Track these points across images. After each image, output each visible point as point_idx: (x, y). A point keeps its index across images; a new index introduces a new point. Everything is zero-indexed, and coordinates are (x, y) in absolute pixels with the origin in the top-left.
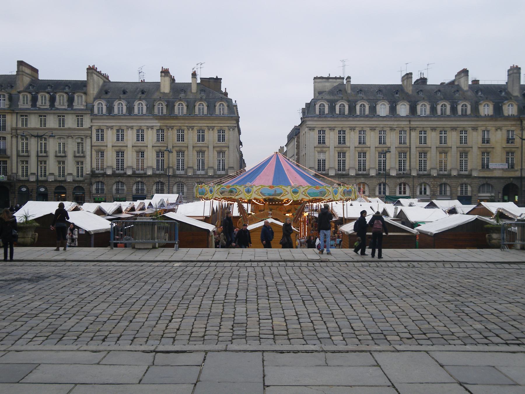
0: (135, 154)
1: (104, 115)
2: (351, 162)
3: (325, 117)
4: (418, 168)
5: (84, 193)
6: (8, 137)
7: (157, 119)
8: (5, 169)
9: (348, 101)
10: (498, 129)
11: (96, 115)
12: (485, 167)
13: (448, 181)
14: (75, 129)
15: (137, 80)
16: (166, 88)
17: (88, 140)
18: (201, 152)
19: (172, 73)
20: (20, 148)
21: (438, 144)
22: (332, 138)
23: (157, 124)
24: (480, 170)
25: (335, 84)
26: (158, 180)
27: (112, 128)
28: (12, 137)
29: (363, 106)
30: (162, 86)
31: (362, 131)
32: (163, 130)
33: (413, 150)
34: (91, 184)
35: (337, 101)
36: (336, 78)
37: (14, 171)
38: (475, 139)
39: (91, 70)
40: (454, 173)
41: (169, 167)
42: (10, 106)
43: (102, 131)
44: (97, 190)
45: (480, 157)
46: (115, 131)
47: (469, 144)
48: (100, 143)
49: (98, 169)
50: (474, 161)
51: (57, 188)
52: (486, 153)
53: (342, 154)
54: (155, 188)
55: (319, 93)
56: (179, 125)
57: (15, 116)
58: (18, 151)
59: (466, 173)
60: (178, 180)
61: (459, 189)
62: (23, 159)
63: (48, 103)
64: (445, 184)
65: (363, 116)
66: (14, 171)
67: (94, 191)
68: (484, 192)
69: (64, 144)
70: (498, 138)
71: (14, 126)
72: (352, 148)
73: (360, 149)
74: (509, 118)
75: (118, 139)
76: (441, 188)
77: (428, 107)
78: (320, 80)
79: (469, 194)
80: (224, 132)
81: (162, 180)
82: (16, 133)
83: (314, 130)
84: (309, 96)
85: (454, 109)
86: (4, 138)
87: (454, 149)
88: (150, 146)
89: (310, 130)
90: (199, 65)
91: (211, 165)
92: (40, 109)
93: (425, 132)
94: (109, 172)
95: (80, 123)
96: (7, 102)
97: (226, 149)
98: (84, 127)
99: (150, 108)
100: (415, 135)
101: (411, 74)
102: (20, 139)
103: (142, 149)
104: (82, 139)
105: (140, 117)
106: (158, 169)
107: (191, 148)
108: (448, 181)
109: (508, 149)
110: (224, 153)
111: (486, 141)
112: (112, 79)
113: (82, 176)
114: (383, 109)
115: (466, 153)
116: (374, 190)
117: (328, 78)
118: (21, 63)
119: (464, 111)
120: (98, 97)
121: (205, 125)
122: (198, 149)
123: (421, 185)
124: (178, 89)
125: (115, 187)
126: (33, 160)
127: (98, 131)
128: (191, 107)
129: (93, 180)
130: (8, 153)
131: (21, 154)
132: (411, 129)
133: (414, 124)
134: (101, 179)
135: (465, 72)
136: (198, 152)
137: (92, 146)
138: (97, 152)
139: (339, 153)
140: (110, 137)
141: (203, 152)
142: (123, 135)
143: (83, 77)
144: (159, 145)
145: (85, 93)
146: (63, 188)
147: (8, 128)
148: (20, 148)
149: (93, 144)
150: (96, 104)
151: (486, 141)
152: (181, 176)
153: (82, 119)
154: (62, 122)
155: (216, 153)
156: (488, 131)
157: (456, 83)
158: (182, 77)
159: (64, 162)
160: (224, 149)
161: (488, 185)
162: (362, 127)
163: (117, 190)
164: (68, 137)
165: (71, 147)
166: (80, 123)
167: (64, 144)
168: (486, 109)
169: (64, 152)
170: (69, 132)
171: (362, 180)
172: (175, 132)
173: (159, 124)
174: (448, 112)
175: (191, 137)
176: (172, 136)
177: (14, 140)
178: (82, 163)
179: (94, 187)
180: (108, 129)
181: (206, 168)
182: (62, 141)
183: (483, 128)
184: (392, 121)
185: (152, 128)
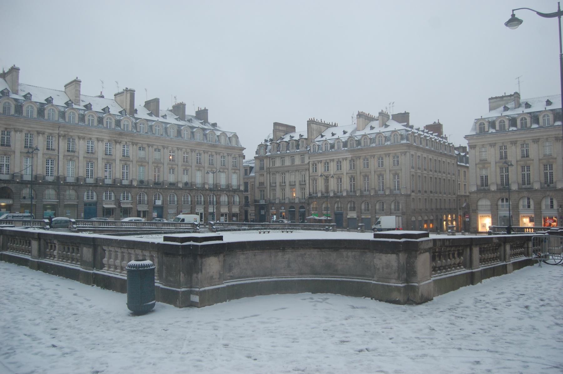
2: (515, 176)
6: (265, 174)
26: (350, 199)
27: (321, 162)
37: (268, 197)
54: (349, 206)
56: (364, 155)
58: (270, 183)
73: (522, 163)
78: (495, 100)
80: (398, 157)
81: (353, 199)
88: (345, 174)
95: (303, 161)
117: (503, 97)
118: (276, 124)
121: (383, 153)
126: (278, 188)
127: (313, 165)
130: (265, 185)
140: (321, 168)
144: (351, 172)
147: (265, 168)
162: (524, 141)
164: (296, 171)
166: (303, 161)
172: (362, 160)
173: (350, 156)
177: (268, 175)
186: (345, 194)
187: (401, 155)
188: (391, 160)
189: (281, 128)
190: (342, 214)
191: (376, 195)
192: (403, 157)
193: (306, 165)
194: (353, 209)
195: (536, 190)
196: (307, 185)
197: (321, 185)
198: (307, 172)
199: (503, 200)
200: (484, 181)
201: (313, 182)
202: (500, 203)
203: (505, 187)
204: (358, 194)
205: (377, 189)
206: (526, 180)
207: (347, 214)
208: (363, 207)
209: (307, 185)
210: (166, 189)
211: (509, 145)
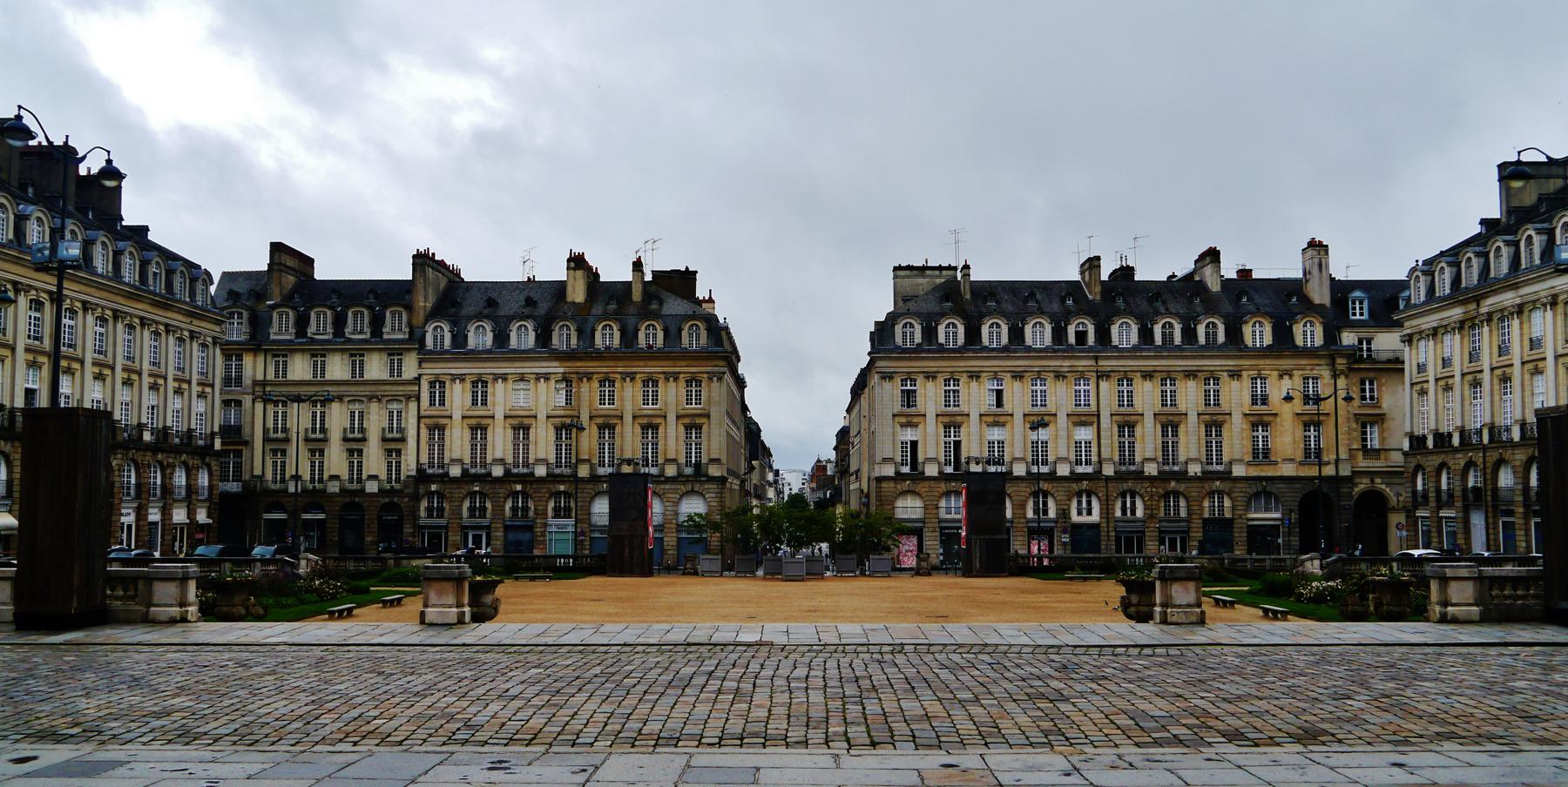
0: (510, 432)
1: (447, 352)
4: (1117, 458)
7: (556, 359)
8: (238, 467)
11: (430, 352)
12: (1262, 455)
13: (1182, 487)
15: (520, 277)
16: (577, 294)
17: (413, 406)
18: (650, 427)
19: (591, 260)
20: (270, 424)
21: (1158, 407)
22: (930, 396)
23: (556, 368)
24: (1249, 464)
25: (939, 281)
27: (462, 378)
28: (253, 401)
30: (569, 288)
34: (416, 498)
36: (940, 268)
38: (1236, 396)
39: (423, 261)
40: (1195, 469)
41: (579, 461)
42: (253, 336)
43: (442, 384)
44: (430, 510)
45: (1248, 434)
46: (468, 385)
49: (431, 465)
50: (1236, 442)
52: (1260, 422)
54: (551, 505)
55: (901, 298)
57: (261, 359)
59: (1220, 468)
61: (1206, 504)
63: (330, 330)
64: (1177, 494)
66: (258, 472)
69: (361, 414)
71: (260, 377)
75: (475, 402)
76: (1167, 501)
77: (1135, 329)
79: (1228, 515)
82: (265, 393)
83: (891, 378)
84: (882, 305)
85: (1189, 334)
86: (239, 403)
87: (1192, 418)
89: (883, 378)
90: (649, 245)
91: (671, 456)
92: (313, 341)
93: (1130, 381)
95: (395, 369)
96: (245, 328)
97: (704, 420)
98: (405, 376)
99: (544, 338)
101: (1098, 258)
106: (558, 464)
107: (628, 418)
108: (1182, 487)
109: (1306, 418)
110: (699, 427)
112: (467, 276)
113: (398, 480)
115: (1219, 426)
117: (923, 269)
118: (277, 249)
120: (436, 313)
122: (645, 421)
123: (1123, 495)
125: (466, 504)
127: (432, 384)
130: (246, 430)
131: (272, 435)
132: (1102, 375)
135: (1212, 255)
137: (419, 418)
138: (431, 429)
140: (458, 398)
141: (655, 428)
142: (485, 394)
143: (406, 273)
145: (409, 308)
146: (358, 506)
147: (247, 381)
149: (423, 413)
153: (400, 361)
154: (358, 368)
155: (682, 429)
156: (1264, 379)
157: (1197, 278)
158: (614, 270)
159: (360, 452)
161: (1268, 495)
164: (370, 398)
166: (395, 369)
167: (361, 414)
168: (1258, 333)
169: (362, 430)
170: (373, 388)
174: (1178, 339)
177: (259, 406)
178: (399, 452)
179: (424, 504)
180: (453, 380)
181: (661, 461)
182: (357, 407)
183: (1254, 373)
184: (1057, 358)
187: (710, 379)
189: (290, 262)
193: (409, 383)
195: (1018, 478)
196: (412, 442)
201: (431, 438)
209: (412, 442)
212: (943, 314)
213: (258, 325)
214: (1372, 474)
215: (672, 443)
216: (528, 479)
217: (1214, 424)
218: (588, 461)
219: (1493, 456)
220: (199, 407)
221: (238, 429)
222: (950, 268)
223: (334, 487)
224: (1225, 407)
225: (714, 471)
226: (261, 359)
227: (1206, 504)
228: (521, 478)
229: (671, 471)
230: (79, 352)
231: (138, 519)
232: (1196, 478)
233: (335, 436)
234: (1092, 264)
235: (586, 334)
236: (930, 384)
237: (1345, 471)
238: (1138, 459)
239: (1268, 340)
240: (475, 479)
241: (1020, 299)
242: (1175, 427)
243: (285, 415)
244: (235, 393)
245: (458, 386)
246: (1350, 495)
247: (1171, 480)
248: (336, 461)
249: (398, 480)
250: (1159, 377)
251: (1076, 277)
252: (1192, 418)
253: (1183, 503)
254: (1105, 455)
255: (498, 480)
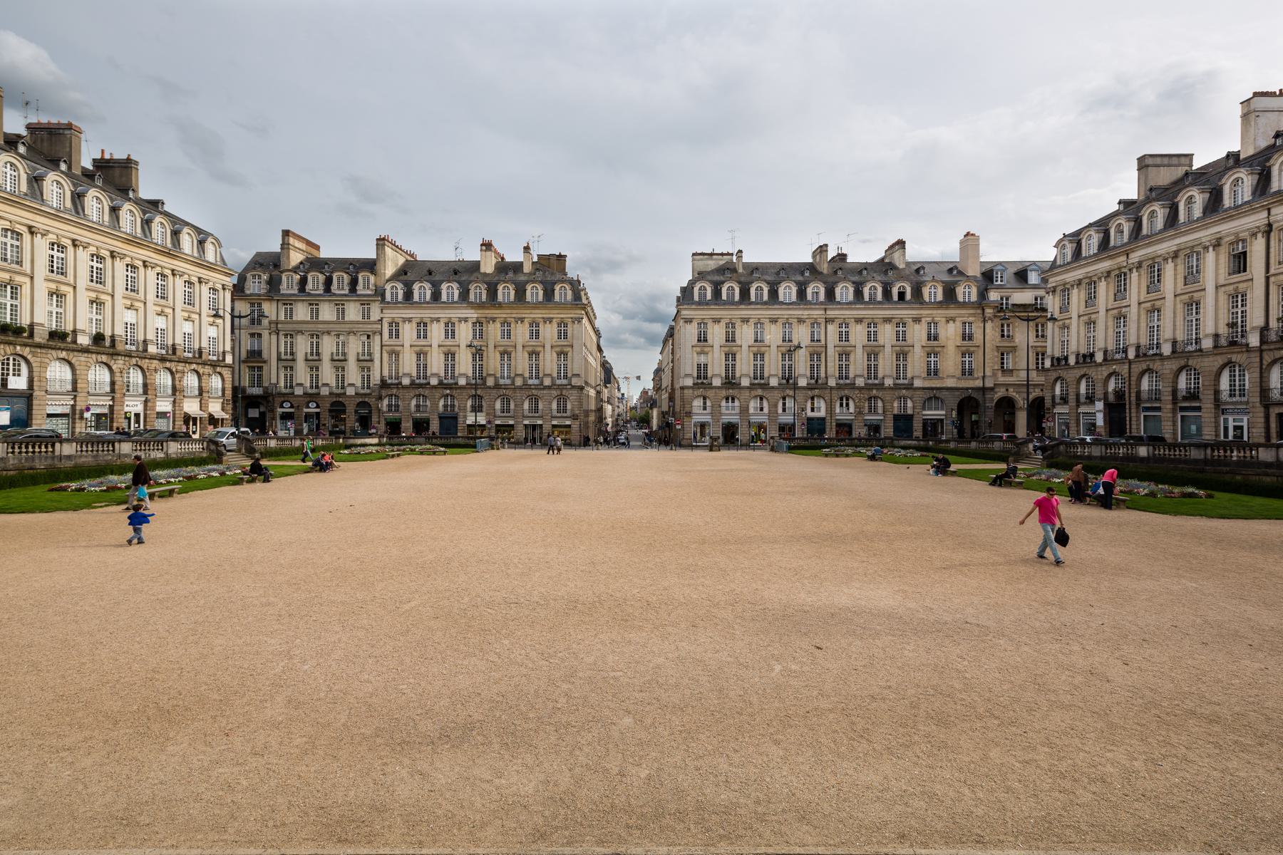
2: (744, 367)
3: (707, 304)
5: (370, 412)
6: (265, 334)
9: (739, 282)
10: (950, 320)
12: (933, 372)
13: (880, 394)
14: (358, 323)
16: (488, 267)
18: (534, 354)
20: (282, 350)
22: (717, 334)
23: (473, 314)
25: (722, 263)
27: (410, 320)
29: (759, 289)
31: (759, 323)
32: (481, 324)
33: (831, 351)
34: (380, 398)
35: (723, 282)
36: (722, 254)
38: (917, 334)
42: (270, 291)
43: (397, 325)
44: (390, 406)
46: (415, 325)
47: (909, 341)
48: (393, 341)
51: (333, 404)
53: (731, 356)
54: (469, 403)
55: (700, 275)
57: (274, 304)
58: (279, 354)
59: (906, 382)
60: (502, 392)
61: (896, 404)
62: (286, 364)
65: (759, 302)
66: (274, 381)
67: (385, 409)
68: (930, 409)
70: (950, 333)
72: (745, 348)
74: (964, 305)
75: (419, 337)
79: (910, 412)
80: (566, 326)
82: (275, 328)
84: (686, 277)
86: (260, 335)
87: (888, 349)
88: (463, 346)
92: (309, 294)
93: (847, 326)
94: (406, 381)
95: (366, 314)
96: (264, 285)
99: (464, 295)
100: (832, 328)
102: (282, 339)
103: (453, 349)
104: (369, 337)
105: (450, 304)
108: (880, 394)
110: (566, 354)
111: (933, 337)
113: (369, 387)
114: (788, 291)
115: (905, 355)
116: (776, 406)
117: (711, 254)
119: (902, 295)
122: (530, 349)
124: (506, 268)
125: (414, 402)
127: (390, 324)
128: (520, 293)
129: (384, 393)
130: (265, 355)
132: (828, 321)
133: (831, 313)
134: (394, 391)
135: (901, 244)
136: (530, 354)
138: (390, 353)
139: (727, 355)
140: (408, 333)
141: (537, 354)
142: (425, 331)
143: (371, 254)
148: (282, 350)
150: (388, 287)
151: (933, 337)
152: (506, 387)
153: (369, 309)
155: (555, 355)
160: (566, 349)
163: (418, 406)
164: (349, 333)
165: (354, 347)
166: (366, 314)
169: (344, 354)
171: (760, 392)
174: (879, 297)
175: (521, 333)
176: (494, 331)
177: (274, 337)
179: (386, 402)
183: (929, 319)
185: (466, 320)
186: (462, 382)
188: (556, 330)
190: (455, 418)
191: (525, 386)
192: (576, 325)
193: (375, 323)
194: (477, 409)
196: (377, 362)
197: (408, 365)
198: (377, 338)
199: (727, 399)
200: (702, 370)
201: (390, 357)
202: (723, 403)
203: (730, 382)
204: (490, 382)
205: (527, 375)
206: (759, 374)
207: (465, 417)
208: (498, 405)
209: (377, 362)
210: (39, 346)
211: (738, 324)
212: (724, 282)
213: (274, 284)
214: (1007, 386)
215: (548, 363)
216: (454, 386)
217: (902, 355)
218: (494, 375)
219: (1137, 368)
220: (212, 332)
221: (260, 353)
222: (728, 254)
223: (325, 391)
224: (909, 341)
225: (575, 381)
226: (274, 304)
227: (896, 404)
228: (449, 386)
229: (547, 382)
230: (70, 279)
231: (145, 409)
232: (890, 388)
233: (326, 357)
234: (823, 249)
235: (492, 292)
236: (716, 326)
237: (989, 384)
238: (851, 375)
239: (940, 297)
240: (419, 386)
241: (778, 273)
242: (876, 355)
243: (292, 343)
244: (256, 329)
245: (407, 326)
246: (992, 399)
247: (873, 389)
248: (328, 375)
249: (369, 387)
250: (866, 321)
251: (811, 260)
252: (888, 349)
253: (880, 404)
254: (830, 371)
255: (434, 387)
